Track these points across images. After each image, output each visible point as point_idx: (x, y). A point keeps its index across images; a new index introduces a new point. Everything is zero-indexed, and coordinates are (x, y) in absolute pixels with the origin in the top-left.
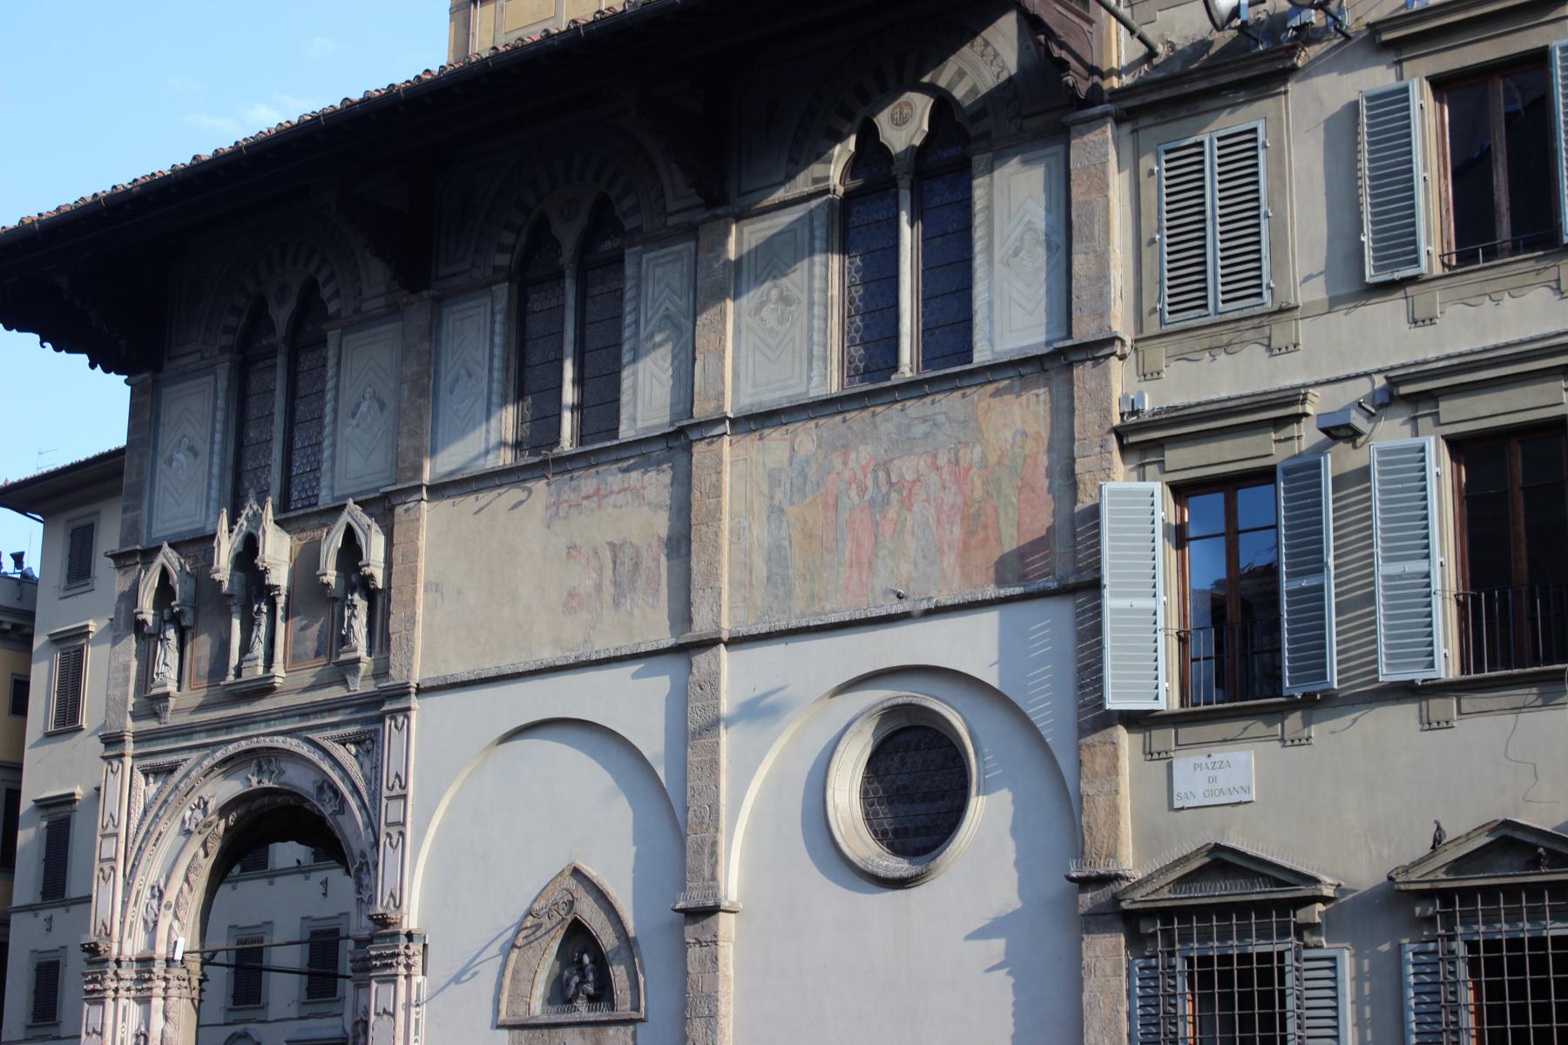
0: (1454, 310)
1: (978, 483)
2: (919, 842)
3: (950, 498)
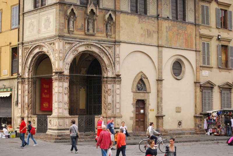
2: (177, 75)
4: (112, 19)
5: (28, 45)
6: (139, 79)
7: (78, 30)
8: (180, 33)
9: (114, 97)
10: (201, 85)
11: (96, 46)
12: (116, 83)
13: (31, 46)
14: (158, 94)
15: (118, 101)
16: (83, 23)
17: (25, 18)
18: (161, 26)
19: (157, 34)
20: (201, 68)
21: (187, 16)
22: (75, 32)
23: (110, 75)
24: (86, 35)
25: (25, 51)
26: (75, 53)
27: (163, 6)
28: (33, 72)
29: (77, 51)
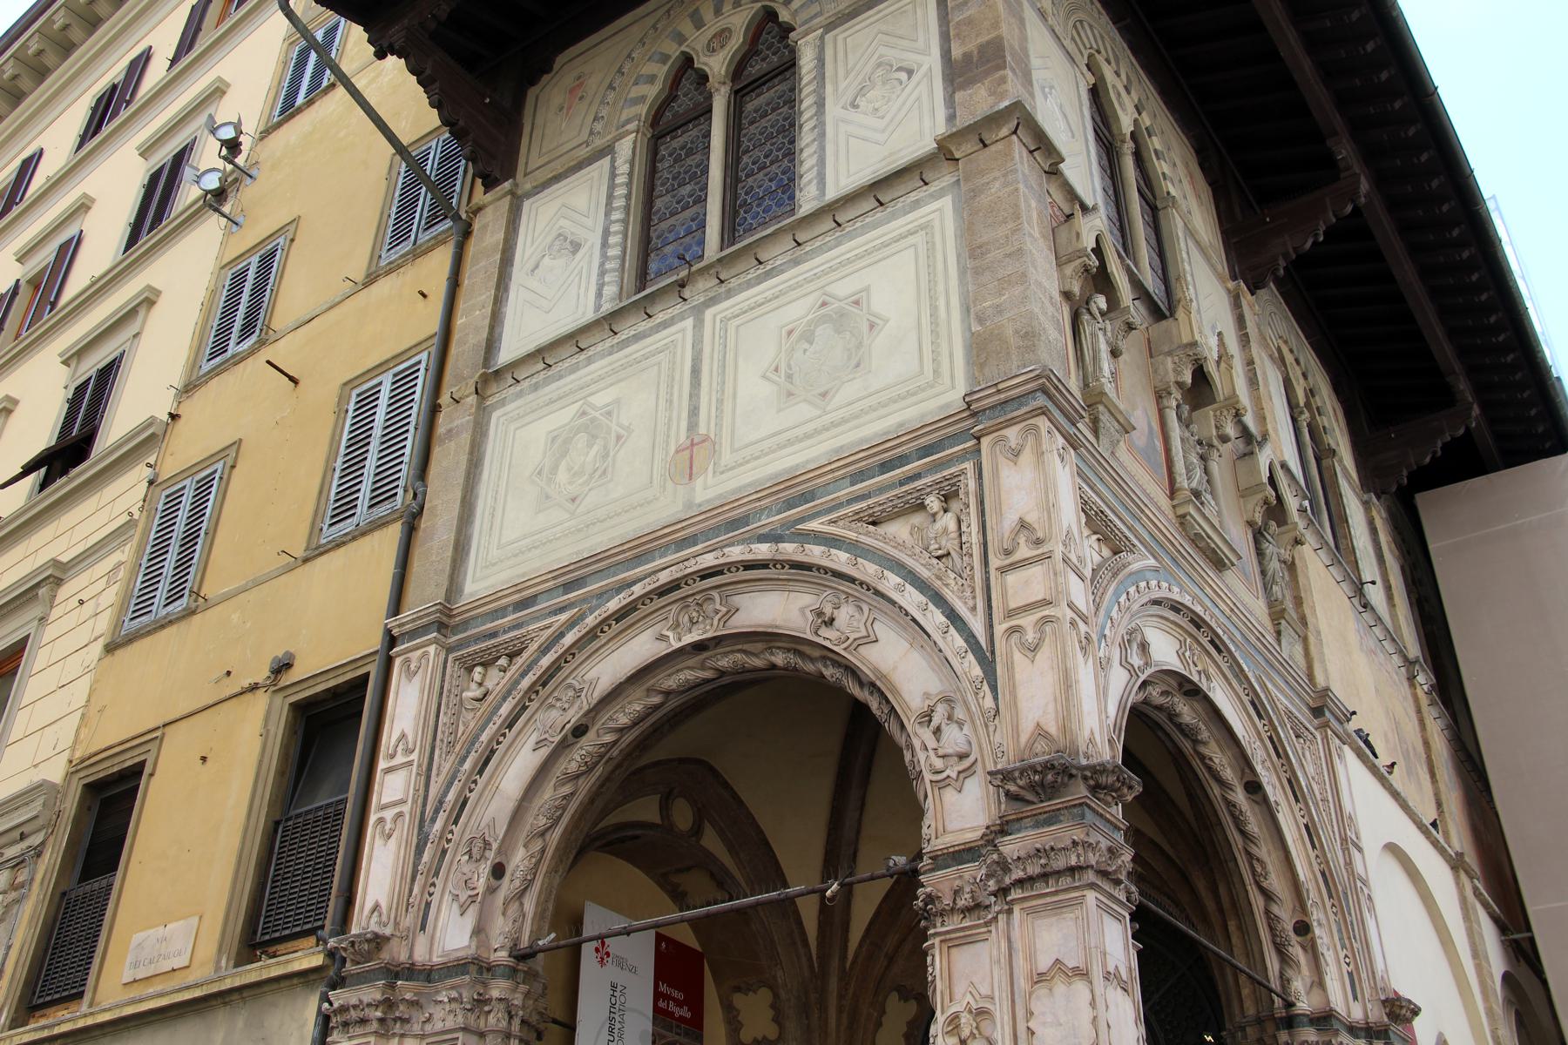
5: (518, 626)
13: (564, 617)
17: (497, 420)
25: (474, 692)
28: (530, 904)
29: (1144, 647)
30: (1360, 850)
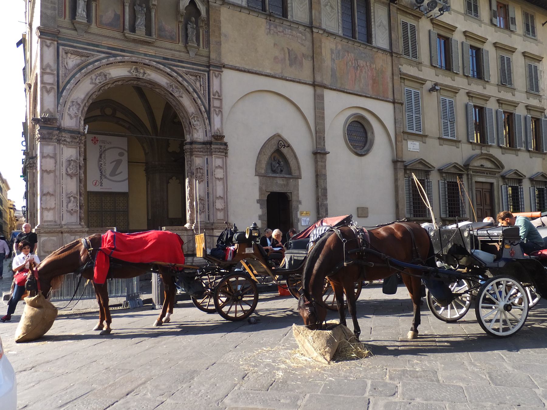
0: (440, 75)
1: (375, 73)
3: (370, 74)
4: (198, 12)
6: (272, 150)
7: (100, 25)
8: (362, 65)
9: (210, 185)
10: (405, 166)
11: (161, 70)
12: (213, 153)
14: (317, 182)
15: (219, 191)
16: (119, 12)
18: (320, 47)
19: (312, 62)
20: (406, 136)
21: (373, 36)
22: (94, 28)
23: (199, 135)
24: (127, 39)
26: (97, 81)
27: (322, 7)
29: (105, 76)
30: (221, 100)
